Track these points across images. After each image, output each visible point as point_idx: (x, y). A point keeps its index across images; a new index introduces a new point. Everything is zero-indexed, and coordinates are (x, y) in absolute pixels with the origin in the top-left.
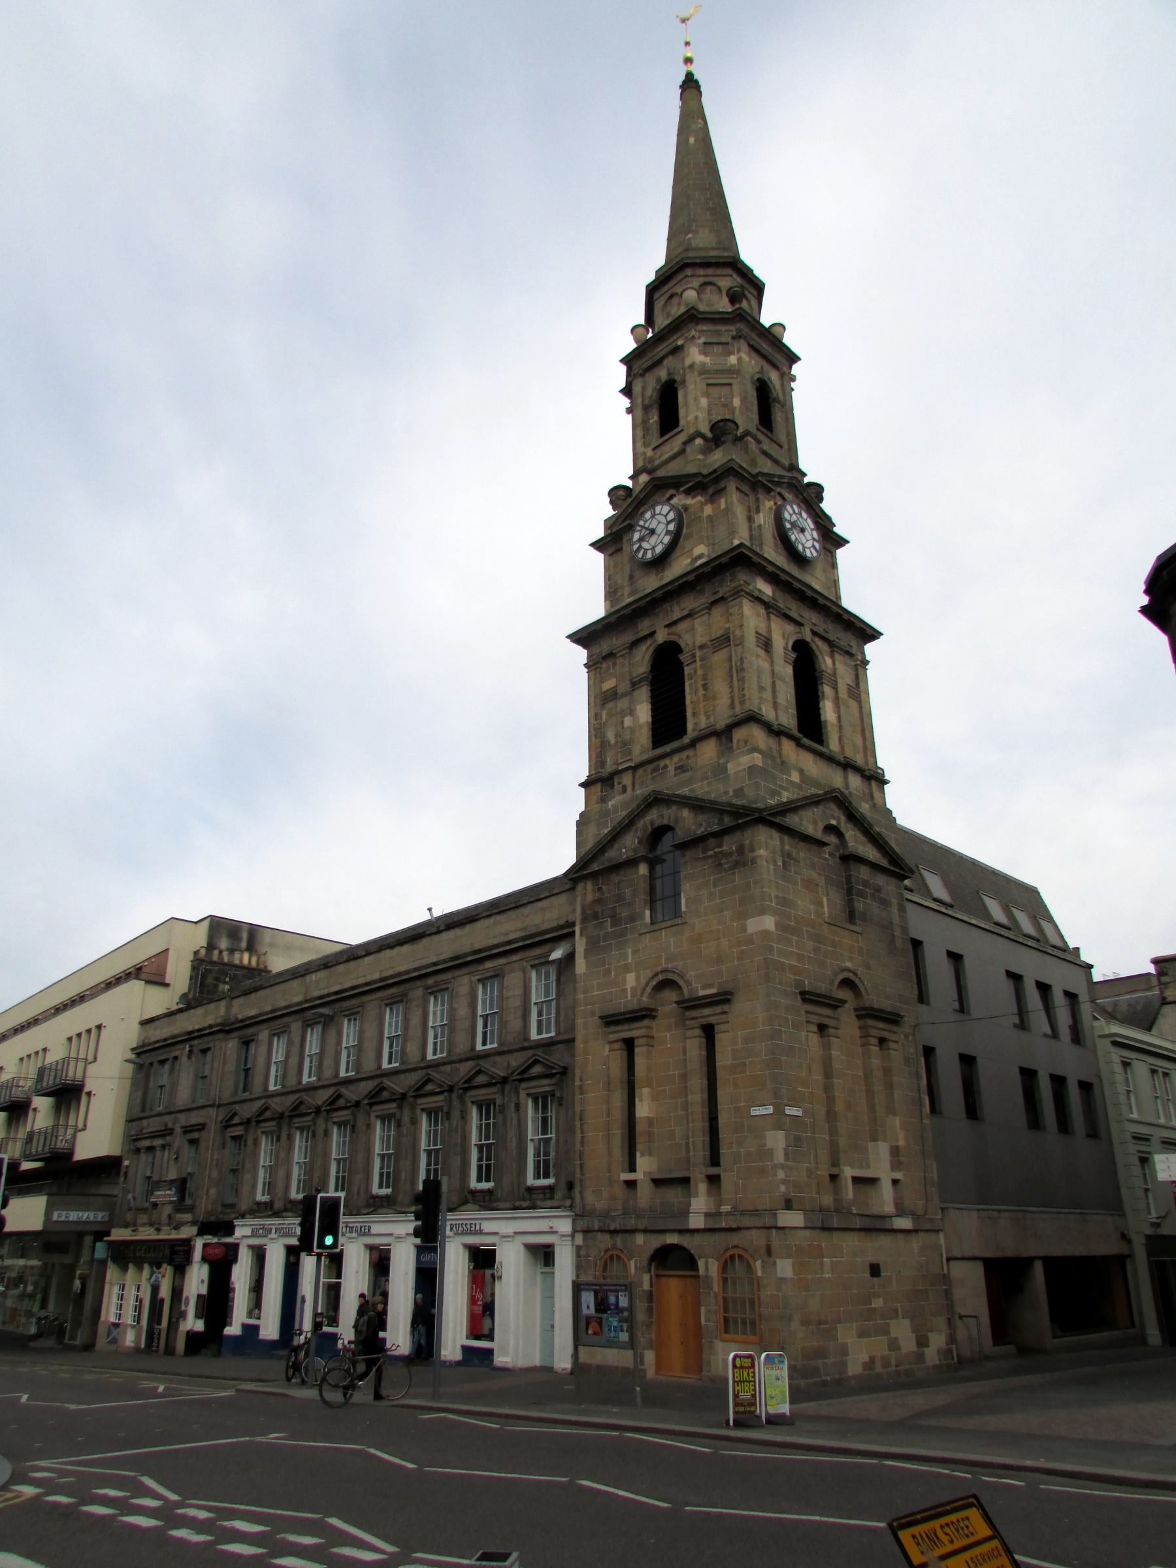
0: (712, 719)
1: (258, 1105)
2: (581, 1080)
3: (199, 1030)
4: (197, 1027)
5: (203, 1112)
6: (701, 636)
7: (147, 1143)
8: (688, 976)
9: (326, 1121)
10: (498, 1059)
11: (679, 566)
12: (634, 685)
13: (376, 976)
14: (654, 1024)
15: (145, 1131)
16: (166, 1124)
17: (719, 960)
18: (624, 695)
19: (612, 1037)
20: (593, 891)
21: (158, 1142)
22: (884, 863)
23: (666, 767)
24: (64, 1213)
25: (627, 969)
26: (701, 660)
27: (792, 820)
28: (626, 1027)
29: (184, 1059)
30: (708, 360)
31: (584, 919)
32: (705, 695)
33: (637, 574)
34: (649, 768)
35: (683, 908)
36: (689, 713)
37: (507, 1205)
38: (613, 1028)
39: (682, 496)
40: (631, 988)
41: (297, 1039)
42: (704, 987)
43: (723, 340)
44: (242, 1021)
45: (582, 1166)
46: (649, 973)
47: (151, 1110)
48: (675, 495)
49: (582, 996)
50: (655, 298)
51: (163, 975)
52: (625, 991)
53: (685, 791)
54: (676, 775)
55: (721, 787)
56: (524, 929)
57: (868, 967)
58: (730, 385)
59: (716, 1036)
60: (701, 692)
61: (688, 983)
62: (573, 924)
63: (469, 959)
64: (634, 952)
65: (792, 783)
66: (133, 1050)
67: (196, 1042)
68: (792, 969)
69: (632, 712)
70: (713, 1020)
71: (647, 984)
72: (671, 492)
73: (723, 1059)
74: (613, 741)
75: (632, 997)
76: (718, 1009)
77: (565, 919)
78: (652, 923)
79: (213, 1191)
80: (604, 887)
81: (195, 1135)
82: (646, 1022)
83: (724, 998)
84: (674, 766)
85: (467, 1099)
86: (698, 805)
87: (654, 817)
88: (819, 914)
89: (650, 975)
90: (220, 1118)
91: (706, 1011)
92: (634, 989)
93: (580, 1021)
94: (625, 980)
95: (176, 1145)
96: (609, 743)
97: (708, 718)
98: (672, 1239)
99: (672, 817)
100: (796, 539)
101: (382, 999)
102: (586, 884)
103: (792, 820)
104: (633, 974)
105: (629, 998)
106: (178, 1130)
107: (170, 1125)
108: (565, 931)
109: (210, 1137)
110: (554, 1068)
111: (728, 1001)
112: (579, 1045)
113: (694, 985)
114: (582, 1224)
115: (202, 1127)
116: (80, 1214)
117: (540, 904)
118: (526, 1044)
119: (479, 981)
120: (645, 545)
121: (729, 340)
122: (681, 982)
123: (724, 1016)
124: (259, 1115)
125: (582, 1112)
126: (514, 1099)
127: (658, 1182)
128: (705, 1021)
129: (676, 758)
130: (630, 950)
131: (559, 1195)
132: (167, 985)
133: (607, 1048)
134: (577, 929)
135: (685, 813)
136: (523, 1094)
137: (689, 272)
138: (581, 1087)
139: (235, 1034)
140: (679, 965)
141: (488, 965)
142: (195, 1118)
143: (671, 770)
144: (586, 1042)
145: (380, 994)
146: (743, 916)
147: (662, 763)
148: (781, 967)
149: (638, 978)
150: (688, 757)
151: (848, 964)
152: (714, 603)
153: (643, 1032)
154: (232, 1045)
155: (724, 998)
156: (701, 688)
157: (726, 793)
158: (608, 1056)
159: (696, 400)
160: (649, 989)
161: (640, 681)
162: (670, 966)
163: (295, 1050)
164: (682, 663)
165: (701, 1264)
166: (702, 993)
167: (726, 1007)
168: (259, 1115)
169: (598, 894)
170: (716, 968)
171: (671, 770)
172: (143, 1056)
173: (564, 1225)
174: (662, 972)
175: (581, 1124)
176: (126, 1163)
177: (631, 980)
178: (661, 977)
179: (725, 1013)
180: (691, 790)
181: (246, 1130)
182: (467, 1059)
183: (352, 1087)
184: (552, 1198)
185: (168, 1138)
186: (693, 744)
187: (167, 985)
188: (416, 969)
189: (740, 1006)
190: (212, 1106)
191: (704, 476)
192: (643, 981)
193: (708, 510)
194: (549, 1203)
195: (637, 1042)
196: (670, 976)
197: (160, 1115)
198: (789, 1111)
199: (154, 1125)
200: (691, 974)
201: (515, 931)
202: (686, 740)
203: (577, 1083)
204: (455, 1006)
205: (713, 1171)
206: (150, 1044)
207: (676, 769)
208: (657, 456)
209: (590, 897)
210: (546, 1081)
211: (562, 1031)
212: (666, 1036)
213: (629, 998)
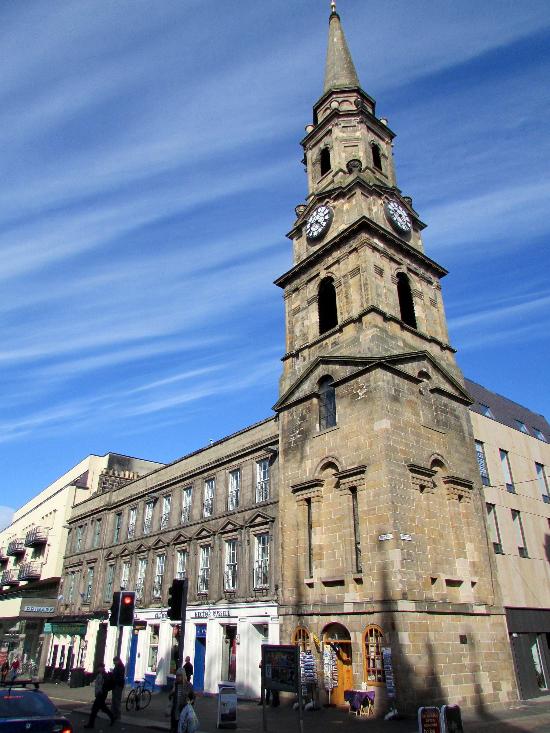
1: (122, 546)
2: (282, 525)
3: (96, 509)
4: (96, 507)
5: (96, 552)
6: (344, 271)
7: (71, 570)
8: (340, 460)
9: (154, 553)
10: (239, 515)
11: (331, 235)
12: (309, 303)
13: (179, 474)
14: (322, 489)
15: (71, 563)
16: (80, 560)
17: (358, 448)
18: (304, 309)
19: (299, 498)
21: (76, 569)
22: (456, 394)
23: (326, 344)
24: (30, 608)
26: (344, 283)
27: (400, 367)
28: (306, 491)
29: (90, 525)
30: (345, 135)
32: (347, 302)
33: (309, 247)
35: (337, 421)
37: (244, 600)
40: (309, 469)
41: (141, 511)
43: (353, 124)
44: (117, 503)
45: (283, 575)
47: (74, 552)
49: (282, 476)
50: (318, 112)
51: (86, 484)
52: (305, 471)
57: (449, 453)
58: (357, 146)
60: (345, 300)
62: (277, 436)
63: (224, 460)
65: (398, 346)
66: (67, 521)
67: (95, 516)
68: (402, 451)
70: (355, 484)
72: (327, 200)
76: (359, 477)
78: (320, 430)
79: (100, 595)
80: (294, 413)
81: (93, 565)
82: (317, 488)
83: (361, 470)
84: (331, 343)
85: (223, 539)
86: (344, 362)
87: (321, 371)
88: (418, 421)
89: (320, 461)
90: (104, 555)
93: (281, 492)
95: (84, 570)
97: (349, 314)
98: (334, 619)
99: (330, 370)
100: (397, 220)
101: (182, 487)
103: (400, 367)
106: (85, 563)
107: (82, 560)
108: (274, 440)
109: (100, 565)
111: (363, 472)
112: (281, 504)
114: (283, 610)
115: (95, 561)
116: (39, 608)
118: (253, 506)
119: (230, 472)
120: (313, 229)
121: (356, 124)
122: (337, 463)
123: (362, 481)
124: (122, 553)
125: (282, 543)
127: (327, 584)
128: (351, 485)
129: (332, 338)
131: (270, 593)
132: (88, 489)
134: (280, 438)
136: (252, 534)
137: (334, 96)
138: (282, 529)
139: (113, 510)
141: (234, 463)
142: (92, 556)
143: (330, 346)
144: (285, 502)
145: (181, 484)
146: (371, 421)
147: (324, 342)
148: (395, 450)
149: (313, 463)
151: (437, 451)
152: (350, 252)
154: (111, 516)
155: (361, 470)
156: (345, 298)
158: (297, 509)
159: (339, 154)
160: (319, 469)
162: (330, 454)
163: (140, 517)
165: (352, 635)
167: (362, 476)
168: (122, 553)
169: (291, 418)
171: (330, 346)
172: (72, 525)
173: (273, 611)
175: (282, 550)
176: (62, 581)
178: (325, 461)
179: (362, 479)
180: (341, 353)
181: (116, 561)
182: (223, 517)
183: (166, 535)
184: (267, 596)
185: (81, 567)
186: (340, 330)
187: (88, 489)
188: (199, 468)
189: (370, 474)
190: (101, 549)
191: (344, 189)
192: (316, 464)
193: (346, 206)
194: (265, 598)
195: (312, 500)
196: (331, 460)
197: (77, 555)
198: (402, 537)
199: (75, 560)
200: (342, 458)
202: (337, 327)
203: (280, 526)
204: (217, 487)
205: (358, 576)
206: (75, 518)
207: (332, 344)
208: (320, 186)
209: (286, 420)
211: (272, 497)
212: (329, 495)
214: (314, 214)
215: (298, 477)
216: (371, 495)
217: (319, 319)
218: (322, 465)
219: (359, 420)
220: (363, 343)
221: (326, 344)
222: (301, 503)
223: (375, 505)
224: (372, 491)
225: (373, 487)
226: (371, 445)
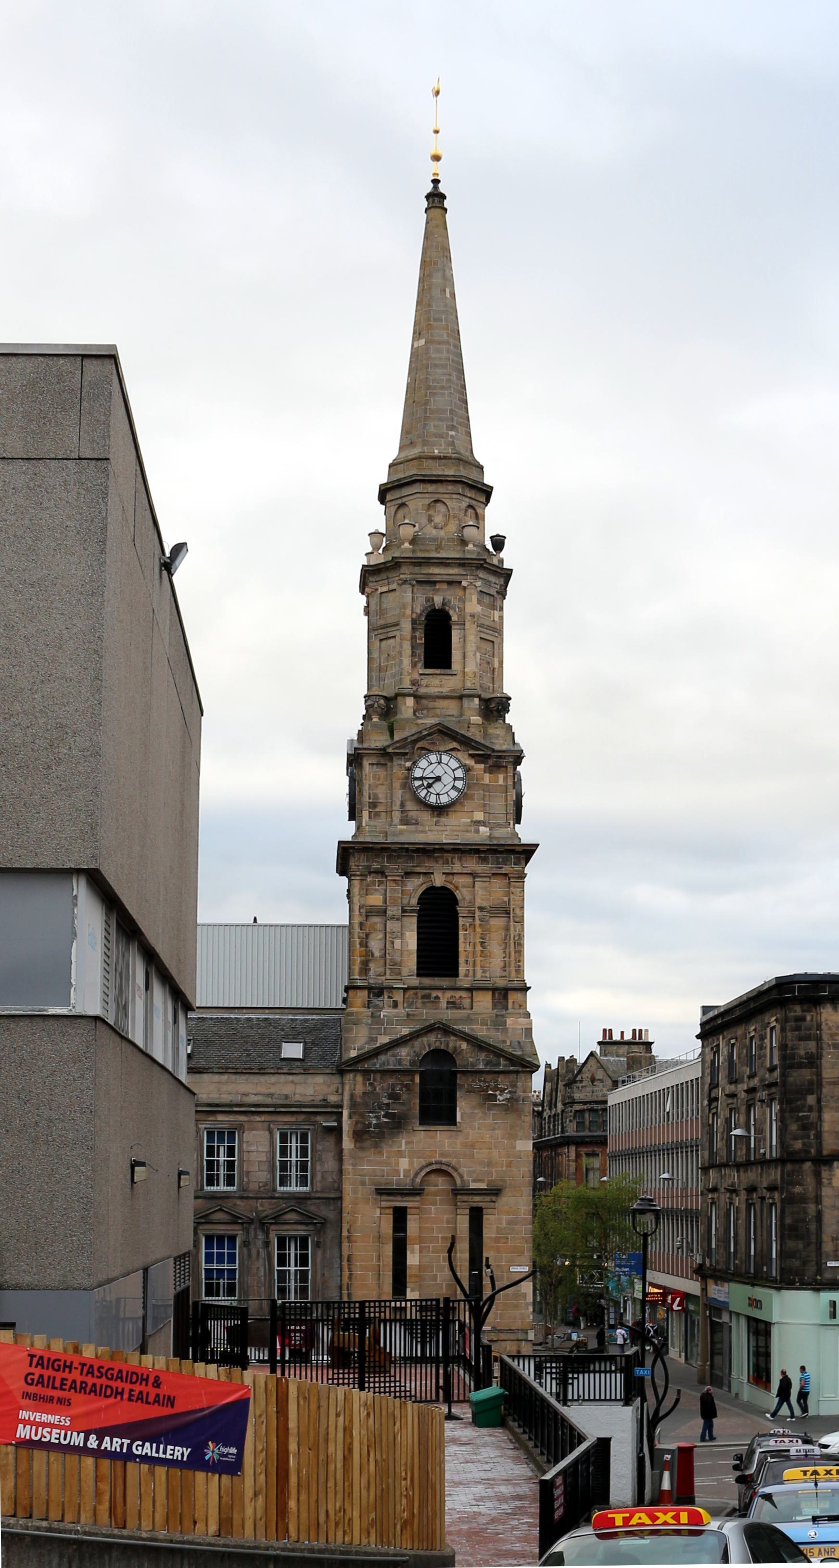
0: (488, 975)
2: (349, 1231)
8: (460, 1171)
17: (489, 1164)
19: (384, 1204)
20: (364, 1084)
25: (400, 1154)
26: (480, 920)
28: (399, 1198)
31: (353, 1105)
34: (421, 993)
35: (458, 1119)
36: (462, 960)
38: (384, 1197)
39: (466, 756)
40: (404, 1170)
42: (475, 1181)
46: (423, 1162)
48: (459, 750)
52: (397, 1172)
53: (466, 1028)
54: (447, 1008)
55: (499, 1036)
56: (271, 1095)
59: (485, 1217)
60: (479, 948)
61: (461, 1177)
64: (407, 1143)
69: (402, 936)
70: (481, 1204)
71: (421, 1169)
72: (455, 745)
73: (488, 1233)
74: (377, 954)
75: (404, 1176)
76: (488, 1198)
77: (321, 1097)
83: (495, 1192)
84: (446, 1000)
86: (478, 1044)
89: (424, 1163)
91: (477, 1198)
92: (406, 1172)
93: (347, 1188)
94: (397, 1164)
96: (373, 955)
97: (484, 972)
99: (451, 1045)
102: (355, 1076)
104: (406, 1160)
105: (402, 1177)
110: (315, 1219)
112: (347, 1204)
113: (465, 1178)
117: (291, 1078)
122: (455, 1174)
126: (261, 1236)
128: (475, 1205)
129: (449, 994)
130: (404, 1141)
133: (378, 1211)
135: (464, 1045)
138: (348, 1237)
140: (454, 1162)
143: (444, 1004)
146: (513, 1137)
147: (434, 994)
149: (411, 1163)
150: (461, 997)
153: (416, 1204)
155: (495, 1192)
156: (479, 944)
157: (505, 1042)
161: (412, 911)
162: (444, 1160)
164: (458, 914)
166: (473, 1186)
167: (494, 1198)
169: (369, 1088)
170: (486, 1169)
174: (436, 1163)
177: (404, 1164)
178: (434, 1167)
179: (494, 1202)
180: (472, 1030)
189: (505, 1200)
191: (493, 751)
192: (417, 1166)
193: (487, 778)
195: (408, 1210)
196: (444, 1167)
200: (463, 1170)
201: (256, 1095)
207: (448, 1003)
209: (360, 1089)
210: (300, 1227)
212: (431, 1208)
213: (402, 1177)
214: (433, 758)
215: (383, 1176)
216: (504, 1222)
217: (418, 945)
218: (428, 1170)
219: (494, 1130)
220: (510, 1031)
221: (437, 997)
222: (388, 1211)
223: (509, 1234)
224: (504, 1218)
225: (508, 1213)
226: (509, 1165)
